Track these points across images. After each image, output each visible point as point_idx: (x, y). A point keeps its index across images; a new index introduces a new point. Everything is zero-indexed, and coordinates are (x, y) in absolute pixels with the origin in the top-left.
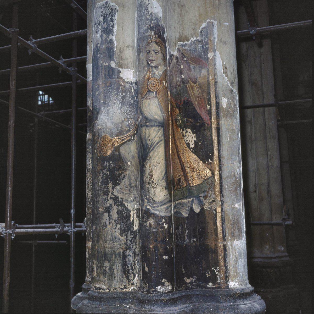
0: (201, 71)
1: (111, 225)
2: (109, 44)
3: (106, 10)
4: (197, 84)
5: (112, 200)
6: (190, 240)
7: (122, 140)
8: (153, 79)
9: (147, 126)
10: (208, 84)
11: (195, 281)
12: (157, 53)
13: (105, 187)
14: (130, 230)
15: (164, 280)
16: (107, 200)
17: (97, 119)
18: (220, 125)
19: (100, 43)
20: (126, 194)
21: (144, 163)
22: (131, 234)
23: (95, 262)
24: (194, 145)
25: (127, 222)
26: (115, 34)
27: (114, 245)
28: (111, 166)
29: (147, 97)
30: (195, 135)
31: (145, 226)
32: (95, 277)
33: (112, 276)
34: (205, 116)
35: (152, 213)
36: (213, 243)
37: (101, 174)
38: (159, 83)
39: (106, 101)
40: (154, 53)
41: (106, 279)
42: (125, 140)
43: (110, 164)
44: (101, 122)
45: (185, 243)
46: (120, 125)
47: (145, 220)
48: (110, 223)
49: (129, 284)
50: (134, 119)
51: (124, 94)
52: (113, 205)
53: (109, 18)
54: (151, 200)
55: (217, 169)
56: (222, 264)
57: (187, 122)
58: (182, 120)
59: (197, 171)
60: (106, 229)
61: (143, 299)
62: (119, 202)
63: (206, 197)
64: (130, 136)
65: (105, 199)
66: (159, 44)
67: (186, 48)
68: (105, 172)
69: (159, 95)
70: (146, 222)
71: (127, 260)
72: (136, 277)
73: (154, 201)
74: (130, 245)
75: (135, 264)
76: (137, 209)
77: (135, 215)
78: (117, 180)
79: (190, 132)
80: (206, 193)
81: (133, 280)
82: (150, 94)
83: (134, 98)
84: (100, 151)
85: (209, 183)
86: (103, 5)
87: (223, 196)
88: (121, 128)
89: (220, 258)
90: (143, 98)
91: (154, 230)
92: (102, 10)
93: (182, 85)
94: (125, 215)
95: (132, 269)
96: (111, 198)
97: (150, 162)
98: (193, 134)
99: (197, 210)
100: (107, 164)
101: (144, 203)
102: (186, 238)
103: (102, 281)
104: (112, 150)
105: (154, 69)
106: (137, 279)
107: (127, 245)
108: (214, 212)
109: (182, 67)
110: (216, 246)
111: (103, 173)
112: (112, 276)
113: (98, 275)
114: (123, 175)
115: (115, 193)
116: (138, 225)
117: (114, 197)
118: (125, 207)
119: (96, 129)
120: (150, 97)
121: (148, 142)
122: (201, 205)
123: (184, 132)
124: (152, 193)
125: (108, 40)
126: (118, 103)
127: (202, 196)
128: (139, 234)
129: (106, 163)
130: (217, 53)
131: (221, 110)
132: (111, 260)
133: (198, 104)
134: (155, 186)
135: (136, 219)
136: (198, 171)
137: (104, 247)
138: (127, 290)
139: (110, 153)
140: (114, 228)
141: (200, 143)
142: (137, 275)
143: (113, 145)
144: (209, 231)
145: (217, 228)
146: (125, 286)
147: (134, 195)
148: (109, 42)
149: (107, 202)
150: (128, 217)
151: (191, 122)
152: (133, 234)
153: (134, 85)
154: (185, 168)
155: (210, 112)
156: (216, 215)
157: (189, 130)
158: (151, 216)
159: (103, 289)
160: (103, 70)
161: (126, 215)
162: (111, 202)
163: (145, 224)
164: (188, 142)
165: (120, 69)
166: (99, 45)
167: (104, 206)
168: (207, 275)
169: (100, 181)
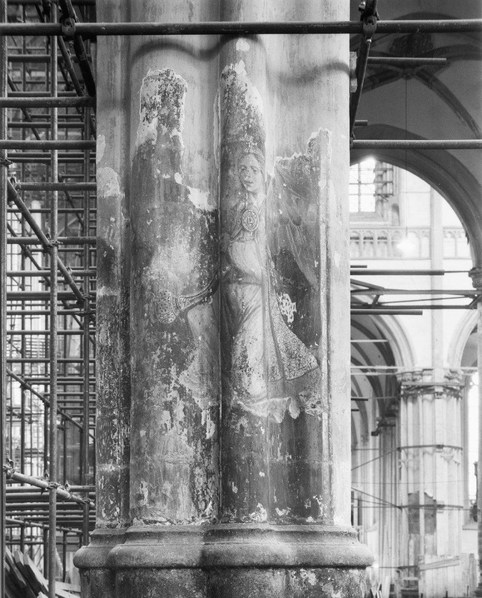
0: (307, 207)
1: (174, 428)
2: (173, 144)
3: (168, 85)
4: (301, 226)
5: (176, 391)
6: (284, 457)
7: (191, 301)
9: (240, 283)
10: (317, 228)
11: (289, 515)
13: (165, 371)
14: (201, 438)
15: (259, 505)
16: (168, 392)
17: (148, 263)
18: (331, 292)
19: (156, 139)
20: (195, 384)
21: (234, 338)
22: (202, 444)
23: (145, 484)
24: (293, 320)
25: (196, 425)
26: (182, 128)
27: (179, 458)
28: (175, 340)
30: (295, 304)
31: (233, 429)
32: (145, 506)
33: (175, 504)
34: (310, 277)
35: (245, 411)
36: (317, 462)
37: (158, 352)
39: (166, 237)
41: (166, 507)
43: (172, 336)
44: (157, 270)
45: (278, 460)
46: (188, 277)
47: (233, 421)
48: (172, 426)
49: (199, 516)
50: (209, 271)
51: (194, 229)
52: (178, 399)
53: (172, 100)
54: (244, 393)
55: (325, 357)
56: (326, 491)
57: (284, 284)
58: (278, 279)
59: (296, 357)
60: (166, 434)
61: (230, 530)
62: (186, 395)
63: (308, 397)
64: (201, 296)
65: (165, 390)
67: (286, 167)
68: (165, 349)
70: (234, 423)
71: (196, 481)
72: (210, 506)
73: (249, 393)
74: (200, 460)
75: (207, 487)
76: (212, 408)
77: (209, 416)
78: (184, 362)
79: (287, 299)
80: (309, 391)
81: (204, 511)
83: (209, 237)
84: (155, 317)
85: (314, 377)
86: (161, 75)
87: (331, 397)
88: (189, 282)
89: (325, 483)
91: (248, 435)
92: (158, 83)
93: (279, 225)
94: (194, 415)
95: (203, 494)
96: (175, 388)
97: (244, 337)
98: (293, 302)
99: (295, 415)
100: (167, 337)
101: (231, 396)
102: (279, 454)
103: (160, 511)
104: (177, 314)
106: (212, 509)
107: (196, 460)
108: (319, 418)
109: (280, 197)
110: (320, 465)
111: (162, 349)
112: (175, 503)
113: (152, 501)
114: (191, 356)
115: (182, 382)
116: (214, 431)
117: (179, 386)
118: (195, 403)
119: (147, 280)
121: (241, 307)
122: (300, 408)
123: (280, 298)
124: (246, 382)
125: (171, 136)
126: (186, 242)
127: (303, 395)
128: (216, 443)
129: (167, 334)
130: (331, 183)
131: (332, 270)
132: (173, 480)
133: (301, 256)
134: (251, 373)
135: (209, 421)
136: (298, 358)
137: (163, 462)
138: (196, 524)
139: (173, 320)
140: (179, 433)
141: (302, 317)
142: (211, 503)
143: (178, 307)
144: (311, 444)
145: (322, 442)
146: (193, 517)
147: (207, 386)
148: (172, 140)
149: (169, 395)
150: (198, 419)
151: (290, 284)
152: (204, 445)
153: (209, 217)
154: (280, 352)
155: (317, 272)
156: (321, 423)
157: (287, 296)
158: (243, 415)
159: (160, 522)
160: (162, 185)
161: (196, 415)
162: (174, 394)
163: (234, 427)
164: (285, 313)
165: (189, 188)
166: (154, 143)
167: (163, 400)
168: (306, 506)
169: (156, 362)
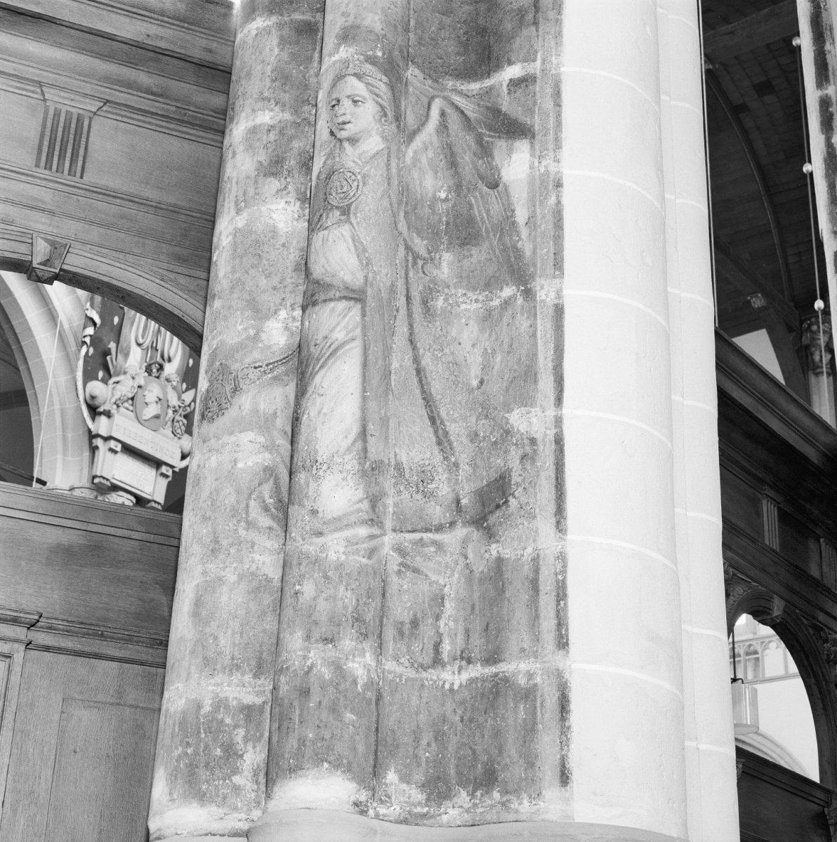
8: (341, 172)
12: (360, 103)
40: (350, 102)
66: (369, 78)
69: (355, 214)
82: (331, 215)
105: (346, 144)
120: (329, 223)
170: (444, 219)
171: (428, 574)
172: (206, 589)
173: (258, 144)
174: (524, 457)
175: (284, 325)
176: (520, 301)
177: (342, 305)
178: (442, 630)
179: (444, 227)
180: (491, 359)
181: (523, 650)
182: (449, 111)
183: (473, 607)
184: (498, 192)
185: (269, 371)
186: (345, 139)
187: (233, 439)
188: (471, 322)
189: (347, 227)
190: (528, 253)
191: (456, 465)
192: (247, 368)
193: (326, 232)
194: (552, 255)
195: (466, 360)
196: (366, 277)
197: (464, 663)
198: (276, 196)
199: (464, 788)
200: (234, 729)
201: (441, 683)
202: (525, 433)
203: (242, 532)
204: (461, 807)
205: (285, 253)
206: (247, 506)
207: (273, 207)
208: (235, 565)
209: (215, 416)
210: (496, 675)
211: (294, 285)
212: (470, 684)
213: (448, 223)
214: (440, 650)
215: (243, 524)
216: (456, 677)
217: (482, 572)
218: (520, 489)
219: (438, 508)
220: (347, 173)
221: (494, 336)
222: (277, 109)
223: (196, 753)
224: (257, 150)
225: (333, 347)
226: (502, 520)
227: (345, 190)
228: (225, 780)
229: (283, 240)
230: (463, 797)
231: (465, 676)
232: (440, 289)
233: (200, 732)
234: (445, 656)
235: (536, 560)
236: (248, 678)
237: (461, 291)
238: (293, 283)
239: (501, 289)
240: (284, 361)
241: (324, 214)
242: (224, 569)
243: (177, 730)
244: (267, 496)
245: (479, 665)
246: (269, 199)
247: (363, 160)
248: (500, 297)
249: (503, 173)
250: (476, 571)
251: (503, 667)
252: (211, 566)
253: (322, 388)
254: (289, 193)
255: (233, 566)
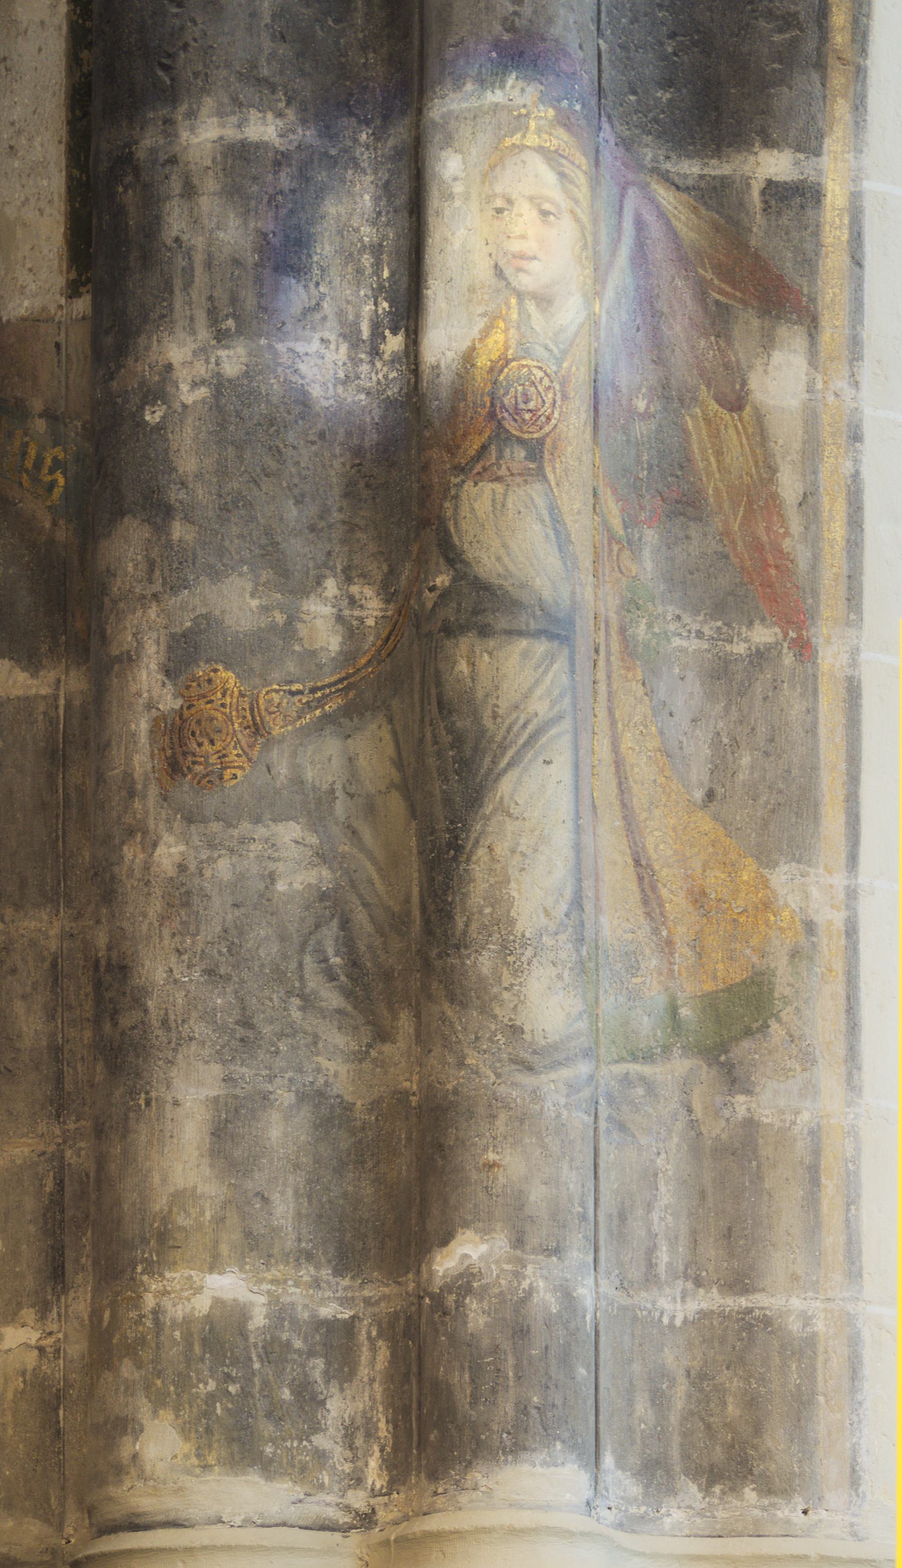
8: (523, 366)
29: (485, 469)
38: (555, 394)
42: (327, 708)
82: (507, 451)
90: (460, 469)
170: (645, 457)
171: (636, 1133)
172: (236, 1111)
173: (255, 188)
174: (794, 954)
175: (334, 610)
176: (788, 659)
177: (541, 647)
178: (656, 1228)
179: (645, 472)
180: (729, 756)
181: (795, 1278)
182: (650, 217)
183: (703, 1195)
184: (741, 420)
185: (313, 704)
186: (529, 293)
187: (261, 831)
188: (690, 675)
189: (538, 486)
190: (803, 565)
191: (669, 943)
192: (277, 691)
193: (499, 487)
194: (845, 580)
195: (681, 748)
196: (573, 593)
197: (690, 1285)
198: (303, 323)
199: (694, 1479)
200: (307, 1358)
201: (657, 1314)
202: (797, 910)
203: (296, 1015)
204: (690, 1507)
205: (327, 454)
206: (301, 965)
207: (300, 347)
208: (290, 1074)
209: (213, 778)
210: (749, 1311)
211: (346, 527)
212: (699, 1319)
213: (650, 468)
214: (654, 1261)
215: (296, 1001)
216: (679, 1306)
217: (718, 1137)
218: (789, 1009)
219: (646, 1018)
220: (535, 371)
221: (734, 715)
222: (291, 114)
223: (245, 1393)
224: (253, 203)
225: (530, 728)
226: (757, 1057)
227: (531, 405)
228: (301, 1440)
229: (321, 424)
230: (691, 1491)
231: (693, 1306)
232: (641, 602)
233: (250, 1359)
234: (662, 1269)
235: (815, 1133)
236: (326, 1273)
237: (671, 610)
238: (344, 522)
239: (751, 624)
240: (340, 686)
241: (493, 447)
242: (271, 1079)
243: (197, 1349)
244: (330, 951)
245: (715, 1290)
246: (289, 327)
247: (562, 346)
248: (747, 640)
249: (754, 382)
250: (706, 1135)
251: (760, 1300)
252: (244, 1070)
253: (517, 804)
254: (325, 318)
255: (287, 1076)
